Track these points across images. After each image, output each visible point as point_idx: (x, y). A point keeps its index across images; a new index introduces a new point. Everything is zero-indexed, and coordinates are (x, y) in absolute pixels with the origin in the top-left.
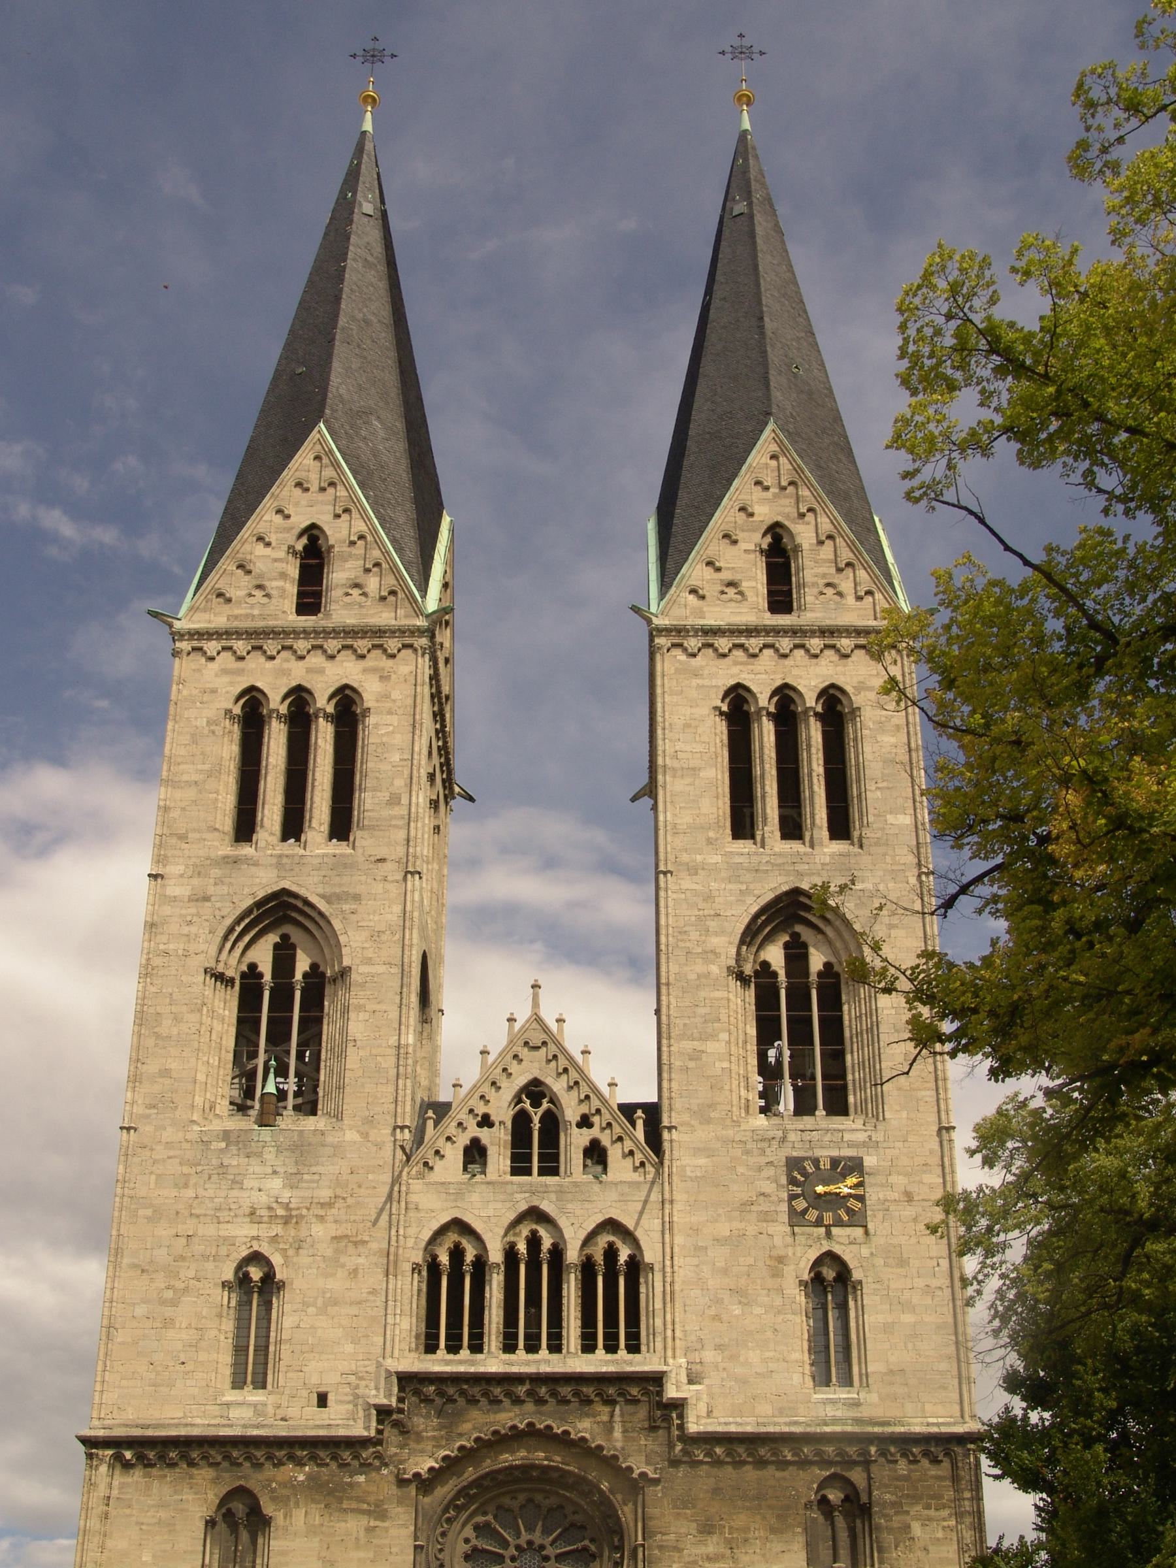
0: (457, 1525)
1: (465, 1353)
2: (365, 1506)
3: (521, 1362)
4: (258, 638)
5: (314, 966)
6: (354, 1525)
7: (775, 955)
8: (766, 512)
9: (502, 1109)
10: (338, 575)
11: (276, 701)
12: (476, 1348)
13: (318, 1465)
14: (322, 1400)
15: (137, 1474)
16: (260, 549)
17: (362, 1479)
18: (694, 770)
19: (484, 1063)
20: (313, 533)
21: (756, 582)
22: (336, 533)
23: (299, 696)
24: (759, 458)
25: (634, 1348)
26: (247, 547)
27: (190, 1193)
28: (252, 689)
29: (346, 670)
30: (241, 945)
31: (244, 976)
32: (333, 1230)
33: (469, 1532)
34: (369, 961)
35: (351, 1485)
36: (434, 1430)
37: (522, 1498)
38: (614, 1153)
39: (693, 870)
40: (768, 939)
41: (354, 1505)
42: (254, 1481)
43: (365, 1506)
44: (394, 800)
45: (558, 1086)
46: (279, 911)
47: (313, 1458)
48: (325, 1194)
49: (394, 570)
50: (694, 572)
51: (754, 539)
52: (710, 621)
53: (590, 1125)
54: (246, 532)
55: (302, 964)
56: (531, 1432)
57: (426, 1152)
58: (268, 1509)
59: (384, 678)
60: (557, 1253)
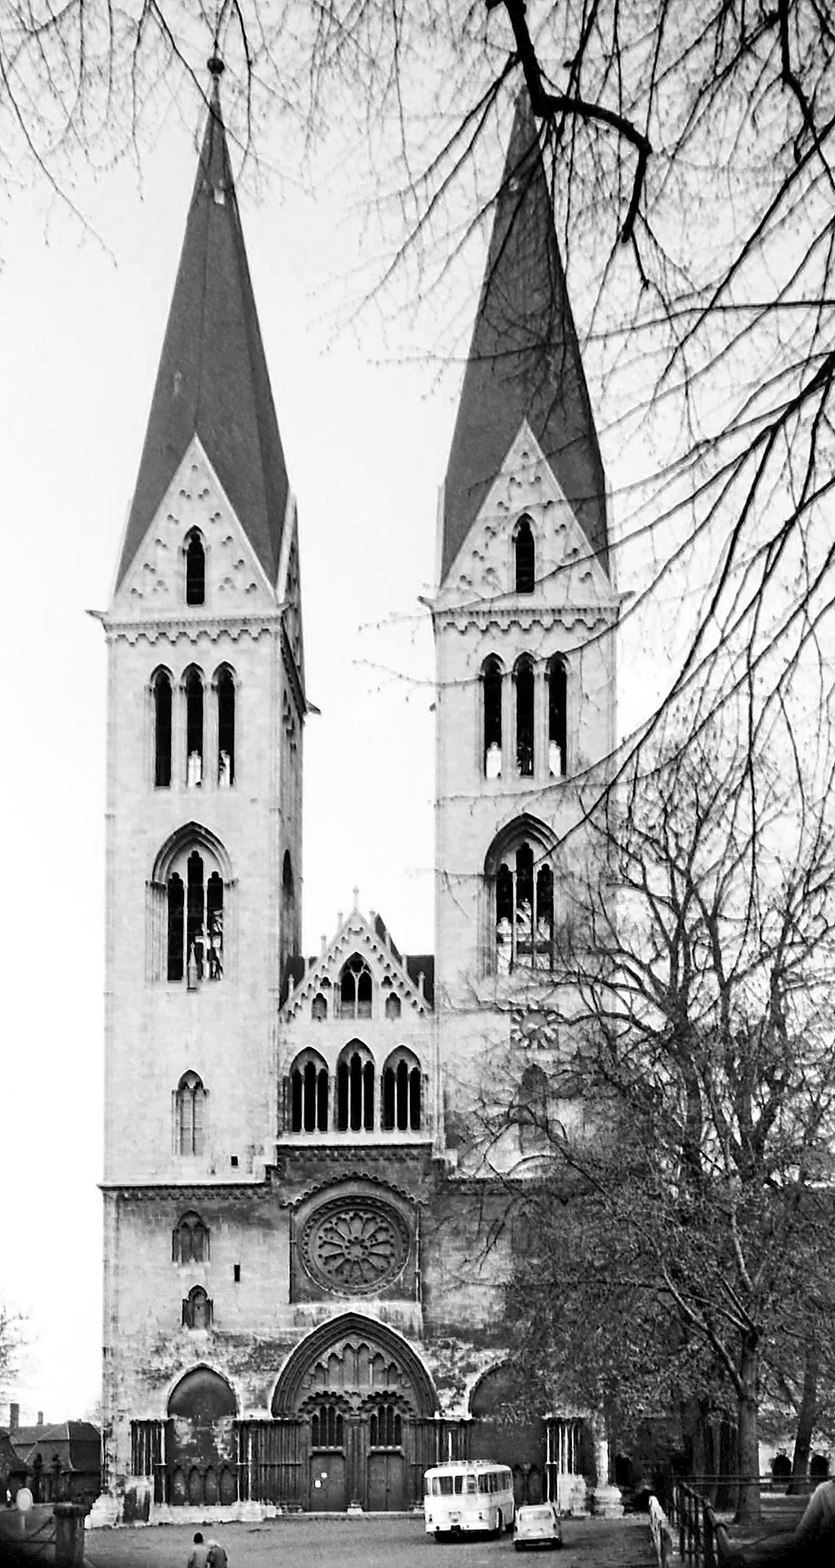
0: (314, 1231)
1: (317, 1131)
3: (350, 1138)
5: (215, 874)
6: (255, 1233)
9: (335, 978)
10: (213, 574)
11: (177, 680)
12: (323, 1128)
14: (235, 1161)
16: (160, 551)
19: (324, 946)
23: (193, 672)
24: (512, 462)
25: (416, 1126)
26: (150, 551)
28: (162, 667)
29: (224, 652)
31: (170, 882)
33: (322, 1234)
34: (249, 875)
37: (351, 1214)
38: (405, 1004)
45: (370, 959)
46: (190, 837)
53: (390, 984)
54: (148, 539)
55: (207, 876)
57: (289, 1006)
60: (370, 1066)
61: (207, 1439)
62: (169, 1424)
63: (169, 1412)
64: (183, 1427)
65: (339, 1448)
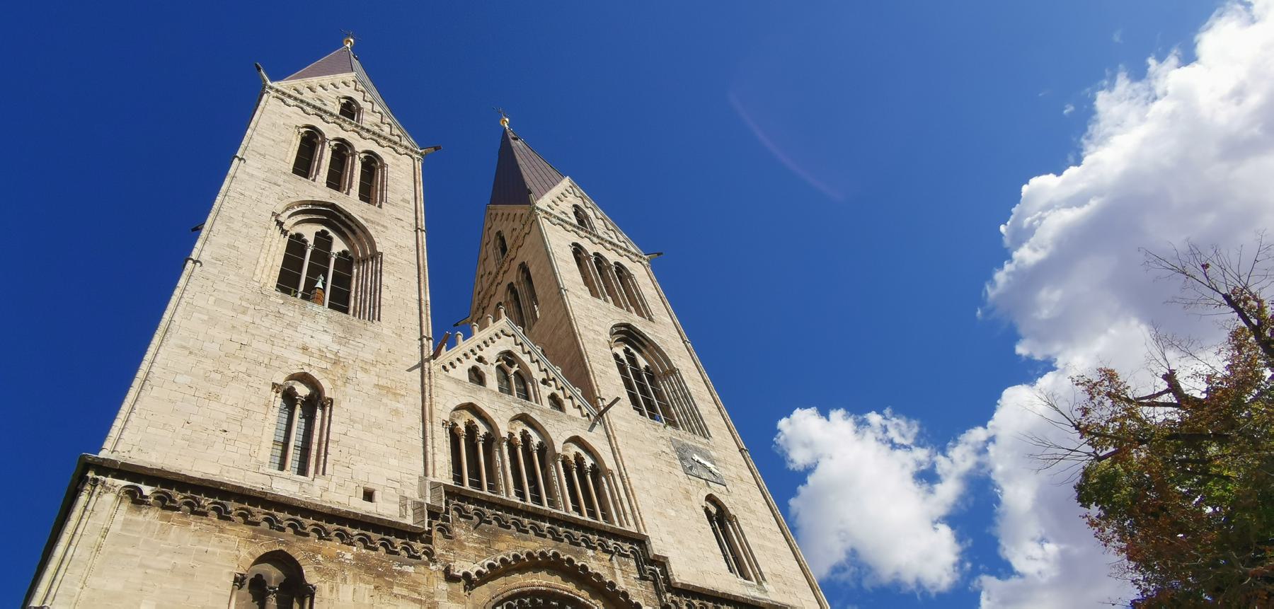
2: (416, 596)
4: (321, 112)
13: (367, 547)
15: (152, 516)
17: (411, 569)
27: (248, 319)
30: (300, 218)
35: (401, 573)
36: (474, 541)
41: (405, 592)
42: (298, 551)
43: (416, 596)
47: (365, 541)
48: (369, 357)
56: (553, 565)
58: (311, 577)
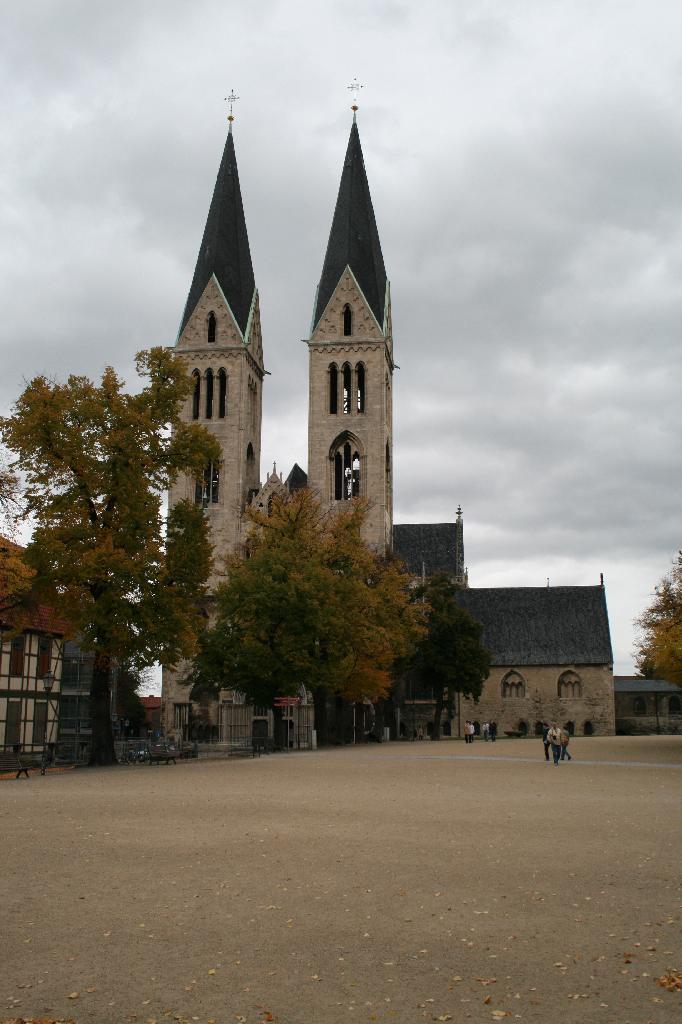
7: (341, 450)
8: (344, 300)
10: (220, 329)
18: (319, 393)
20: (212, 314)
21: (340, 324)
22: (218, 314)
29: (222, 363)
32: (222, 538)
34: (229, 457)
39: (318, 426)
40: (340, 445)
44: (236, 405)
49: (235, 327)
50: (322, 324)
51: (340, 310)
52: (326, 342)
59: (233, 365)
61: (206, 713)
62: (190, 705)
63: (190, 699)
64: (196, 706)
65: (265, 718)
